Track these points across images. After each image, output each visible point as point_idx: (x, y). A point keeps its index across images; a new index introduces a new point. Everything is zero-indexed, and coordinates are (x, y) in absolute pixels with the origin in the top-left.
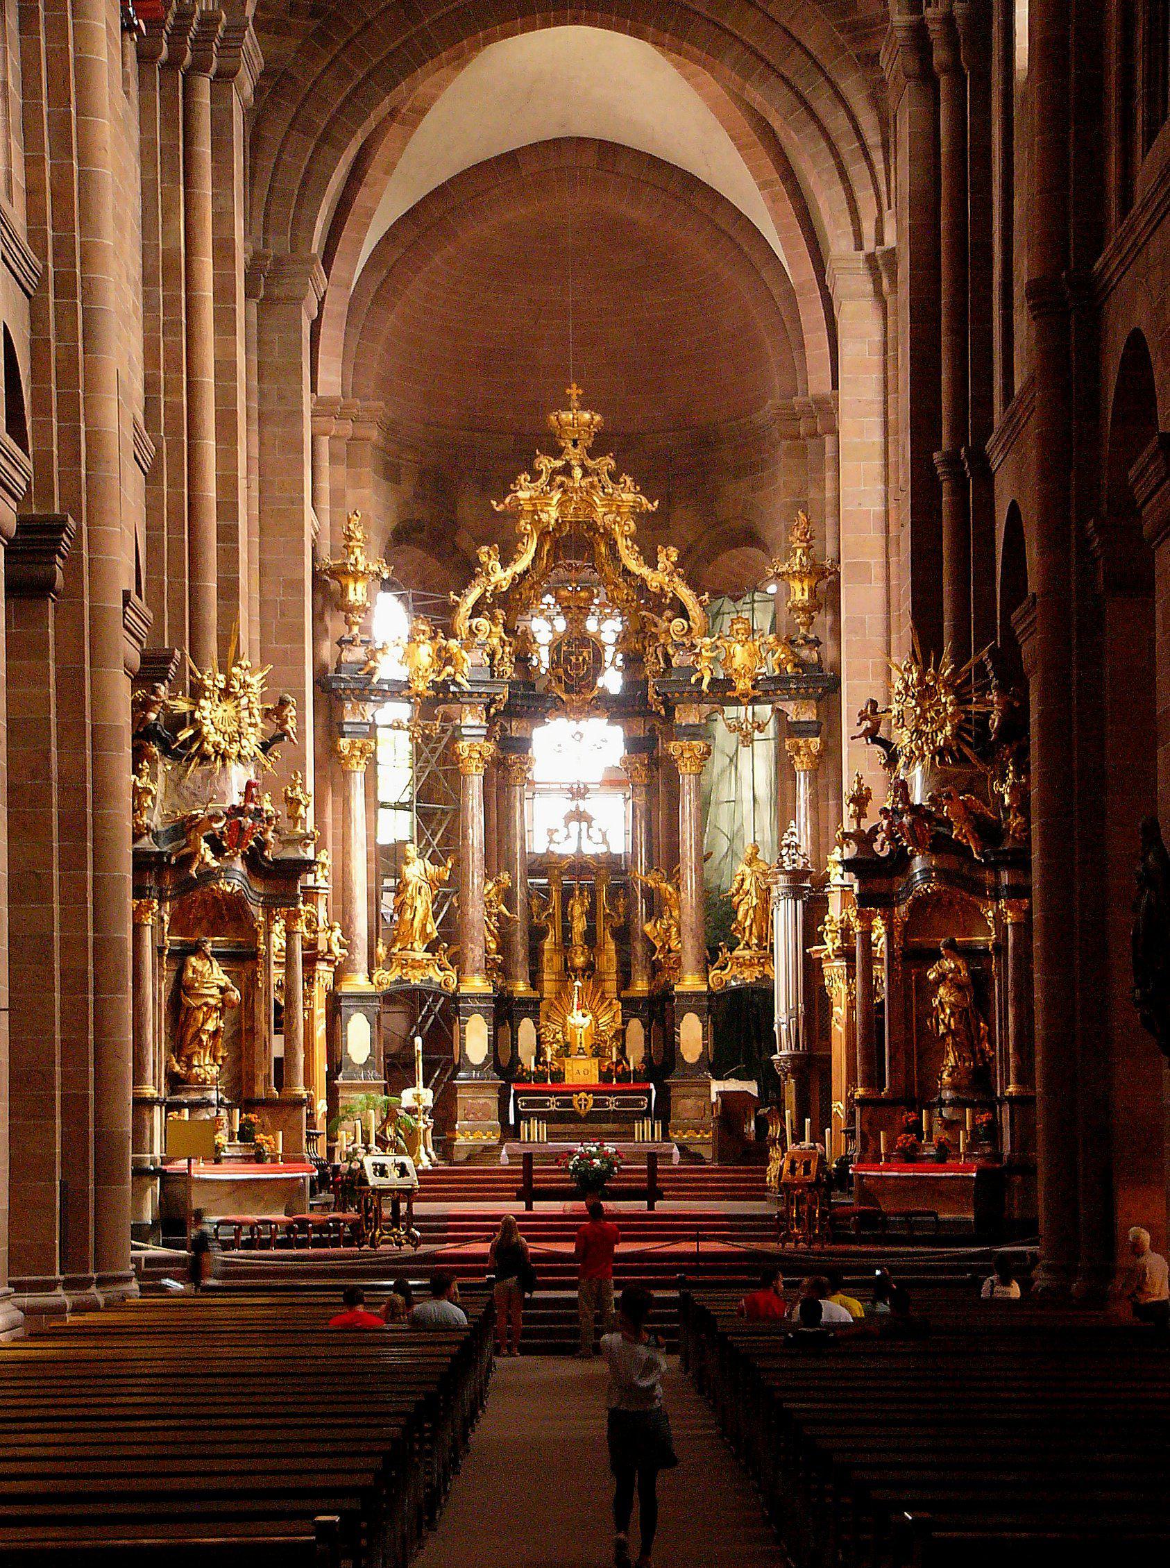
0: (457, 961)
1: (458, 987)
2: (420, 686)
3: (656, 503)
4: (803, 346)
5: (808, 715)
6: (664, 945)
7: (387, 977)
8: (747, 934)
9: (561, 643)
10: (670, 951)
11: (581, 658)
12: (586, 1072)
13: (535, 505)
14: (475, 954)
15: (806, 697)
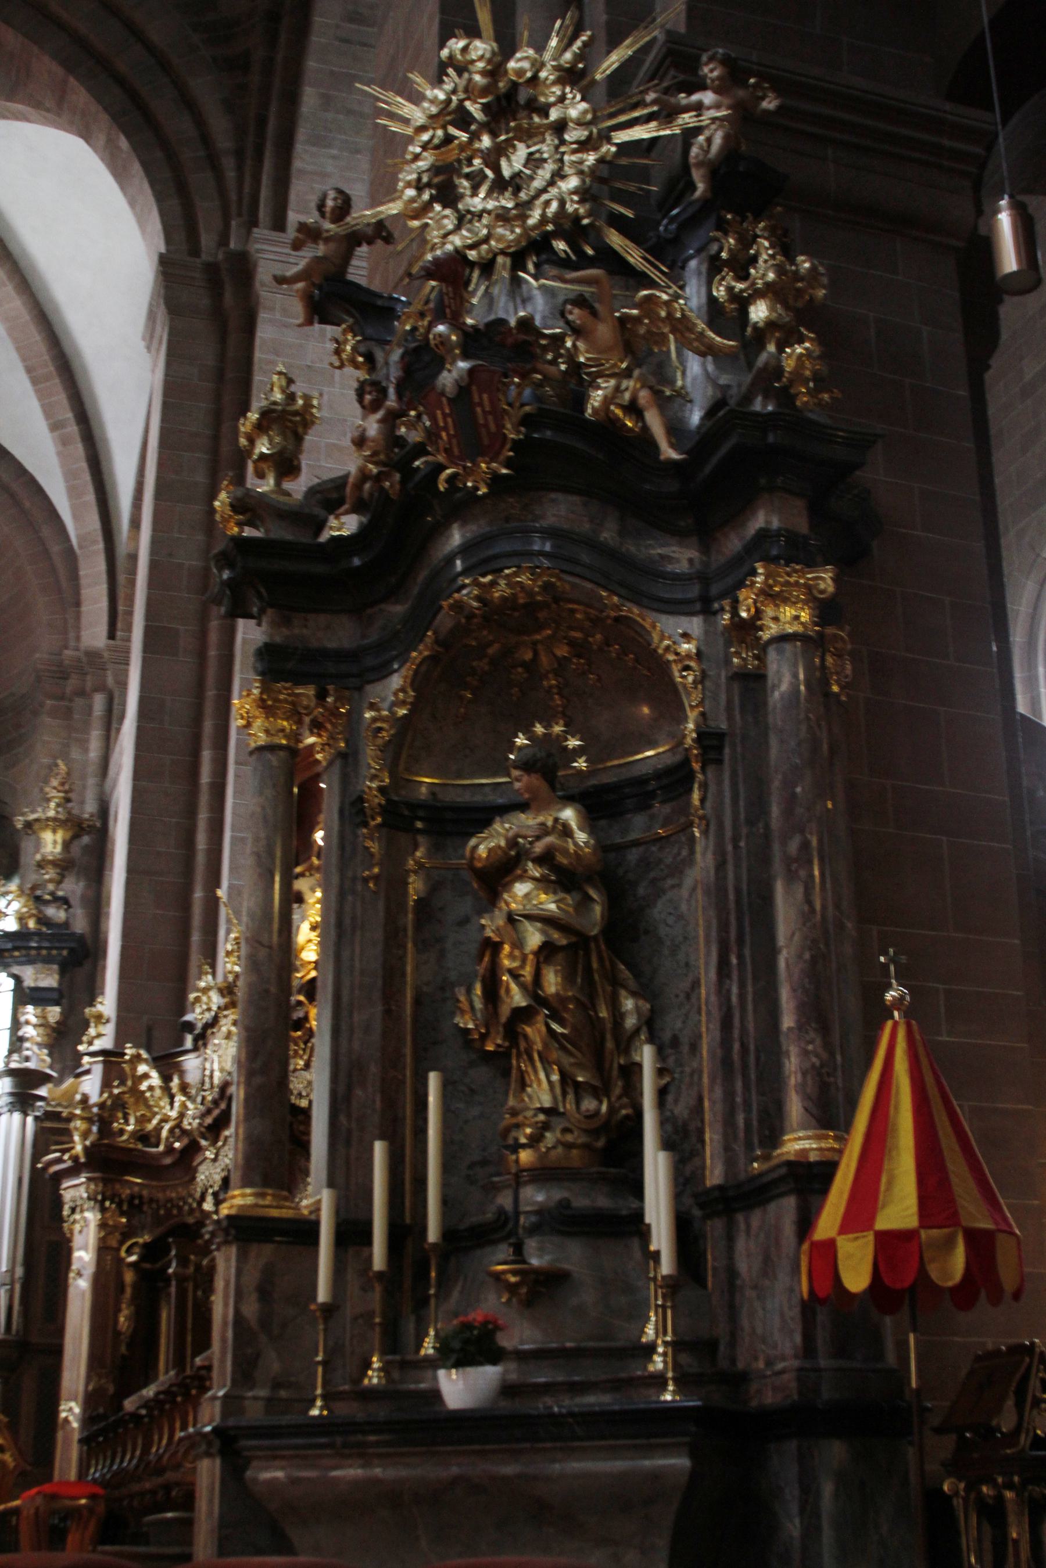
4: (78, 604)
5: (49, 980)
15: (48, 960)
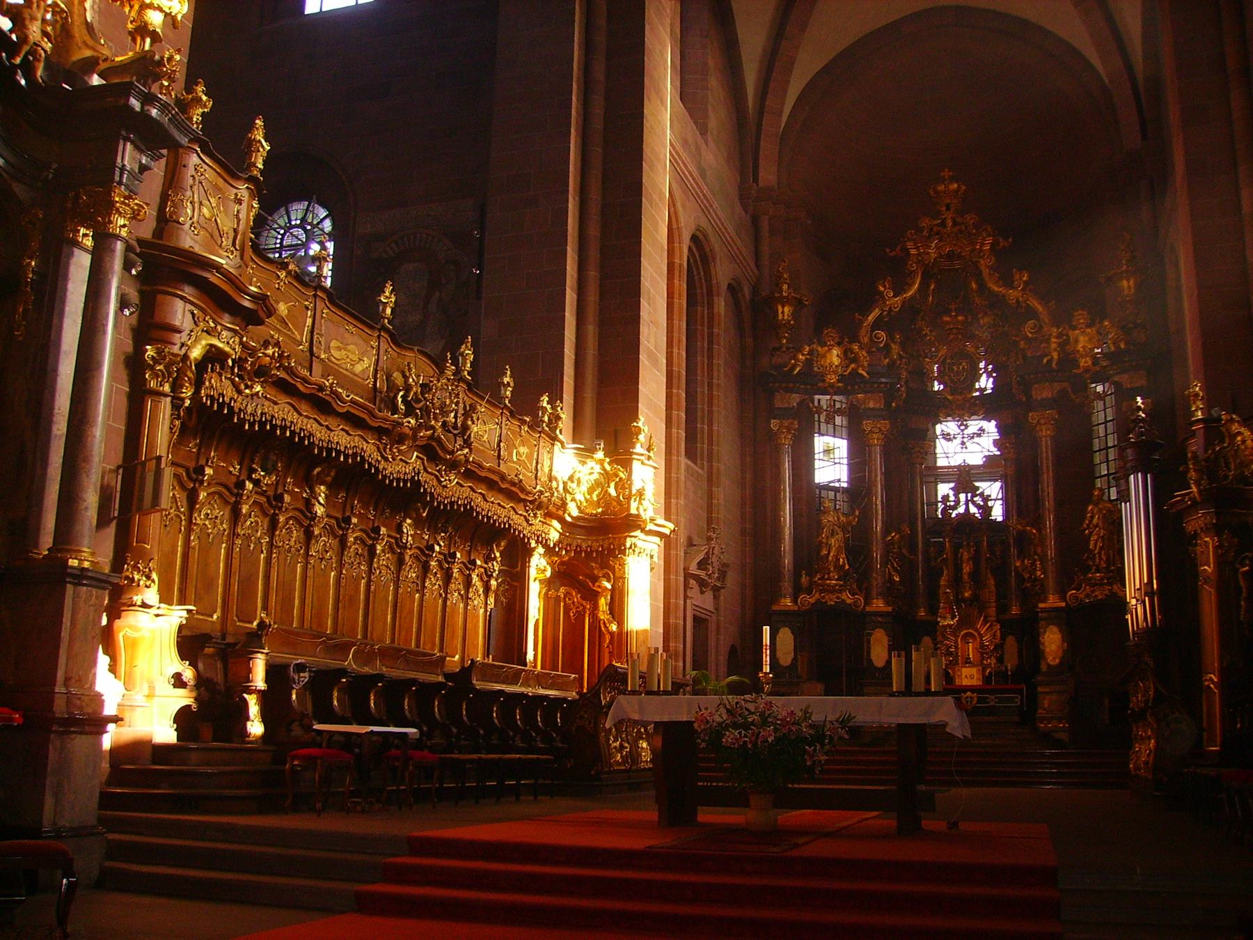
0: (862, 585)
1: (864, 606)
2: (832, 379)
3: (1010, 240)
6: (1031, 576)
7: (808, 599)
8: (1097, 560)
9: (945, 359)
10: (1036, 580)
11: (961, 367)
12: (972, 677)
13: (917, 248)
14: (877, 580)
